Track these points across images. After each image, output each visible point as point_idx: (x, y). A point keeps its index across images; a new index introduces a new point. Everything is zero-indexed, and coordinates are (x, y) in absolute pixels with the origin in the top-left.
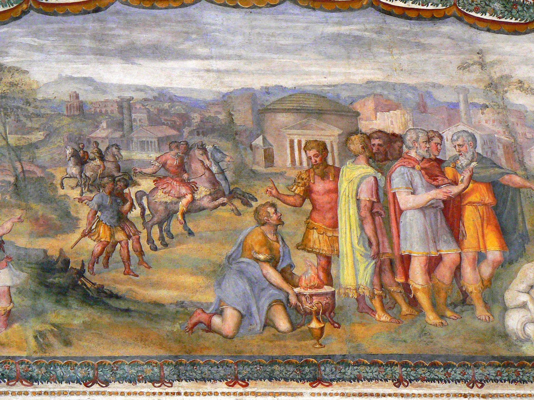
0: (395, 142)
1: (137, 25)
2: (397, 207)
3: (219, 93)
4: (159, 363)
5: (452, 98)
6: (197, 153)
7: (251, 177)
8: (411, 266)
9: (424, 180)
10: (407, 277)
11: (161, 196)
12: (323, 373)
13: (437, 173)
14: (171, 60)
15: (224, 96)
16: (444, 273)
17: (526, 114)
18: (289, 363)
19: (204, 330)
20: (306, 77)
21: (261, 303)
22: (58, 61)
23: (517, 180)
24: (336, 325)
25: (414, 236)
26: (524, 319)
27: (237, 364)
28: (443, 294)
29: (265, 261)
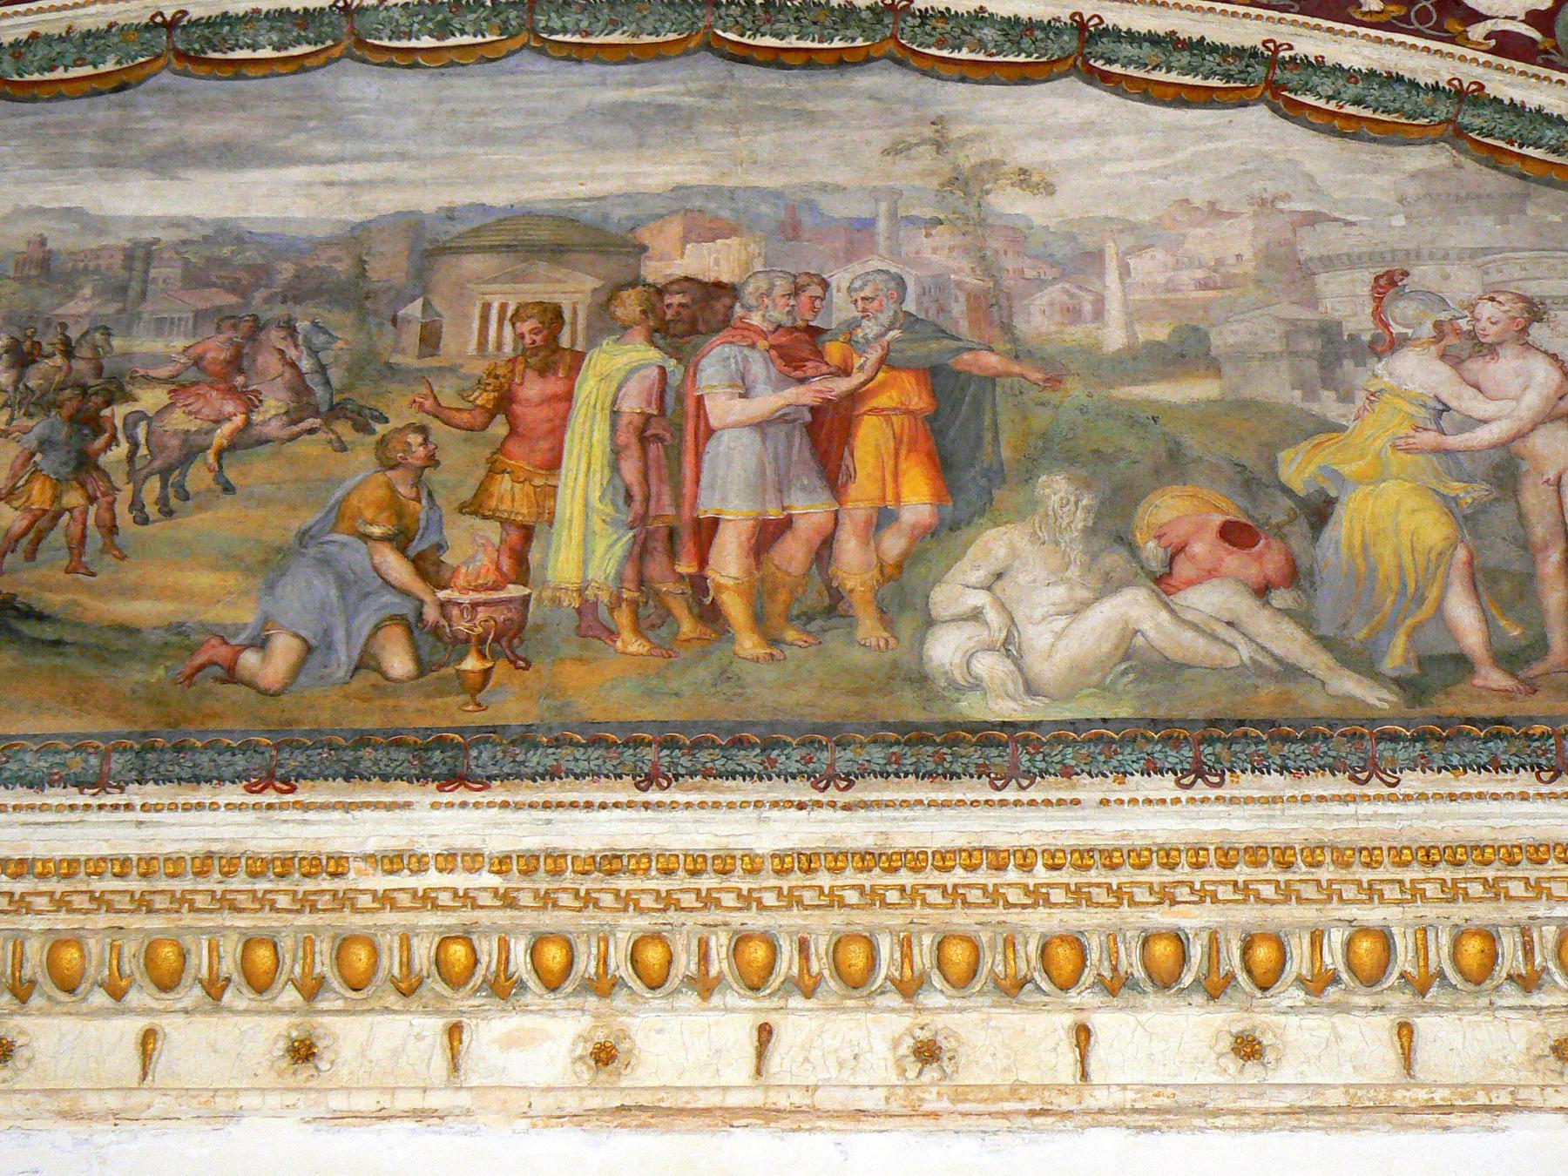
0: (718, 298)
1: (197, 110)
2: (702, 425)
3: (346, 223)
4: (103, 747)
5: (863, 211)
6: (275, 337)
7: (385, 377)
8: (718, 541)
9: (773, 370)
10: (703, 561)
11: (179, 420)
12: (473, 763)
13: (806, 354)
14: (257, 167)
15: (353, 229)
16: (792, 553)
18: (398, 744)
19: (216, 679)
20: (542, 184)
21: (357, 623)
22: (18, 182)
23: (992, 360)
24: (521, 663)
25: (731, 481)
26: (971, 644)
27: (278, 747)
28: (782, 596)
29: (384, 539)
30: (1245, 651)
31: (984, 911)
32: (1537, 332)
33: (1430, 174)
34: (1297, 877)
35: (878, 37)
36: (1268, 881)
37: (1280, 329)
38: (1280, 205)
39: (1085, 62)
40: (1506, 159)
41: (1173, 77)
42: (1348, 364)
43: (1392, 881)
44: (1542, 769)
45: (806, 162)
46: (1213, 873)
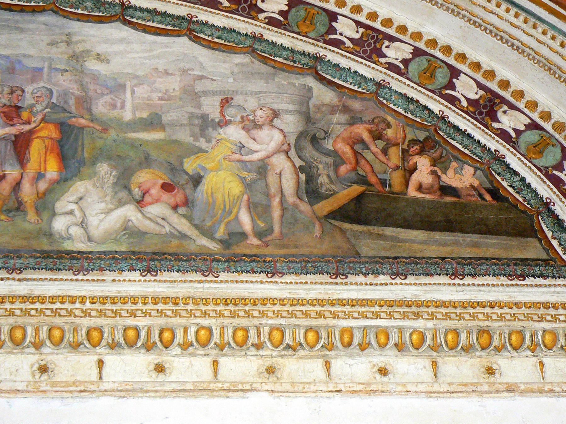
5: (39, 65)
13: (14, 116)
17: (98, 76)
23: (83, 121)
26: (69, 223)
30: (168, 229)
31: (66, 318)
32: (276, 122)
33: (242, 65)
34: (180, 308)
35: (48, 3)
36: (170, 310)
37: (187, 116)
38: (190, 72)
39: (123, 17)
40: (269, 61)
41: (155, 25)
42: (210, 129)
43: (213, 310)
44: (268, 273)
45: (18, 46)
46: (150, 306)
